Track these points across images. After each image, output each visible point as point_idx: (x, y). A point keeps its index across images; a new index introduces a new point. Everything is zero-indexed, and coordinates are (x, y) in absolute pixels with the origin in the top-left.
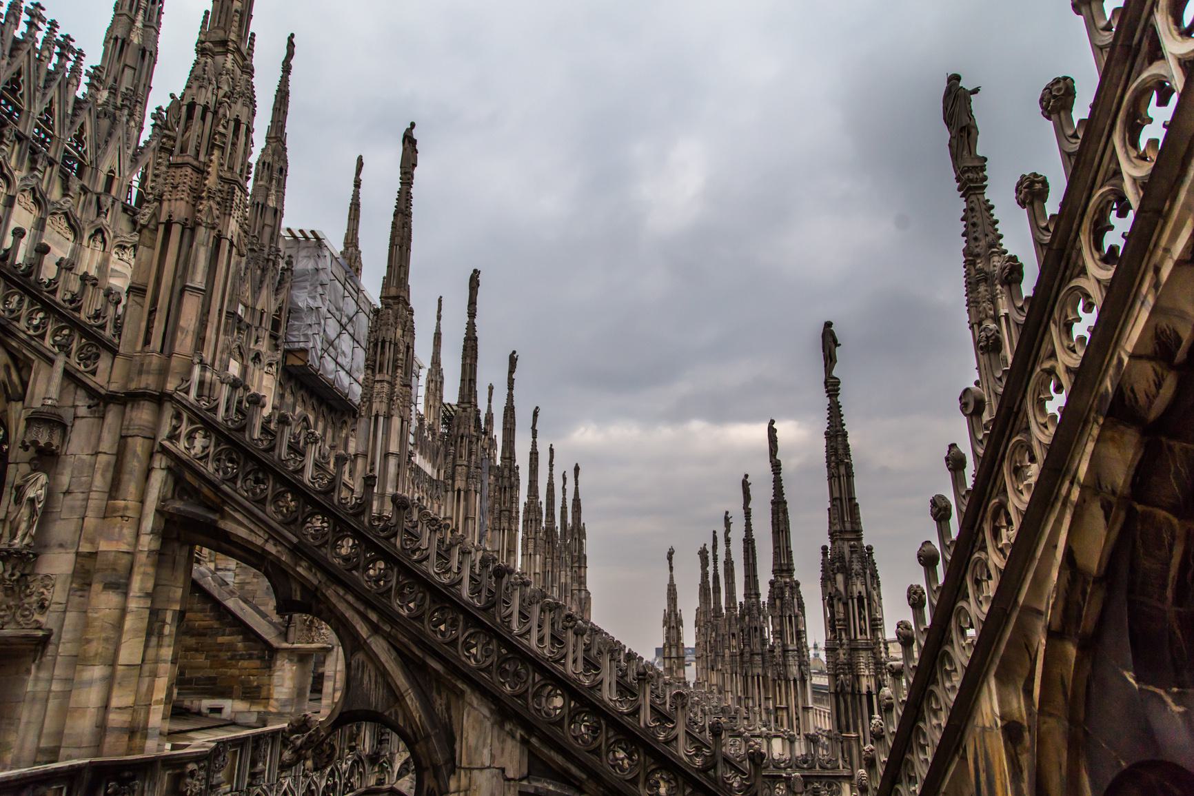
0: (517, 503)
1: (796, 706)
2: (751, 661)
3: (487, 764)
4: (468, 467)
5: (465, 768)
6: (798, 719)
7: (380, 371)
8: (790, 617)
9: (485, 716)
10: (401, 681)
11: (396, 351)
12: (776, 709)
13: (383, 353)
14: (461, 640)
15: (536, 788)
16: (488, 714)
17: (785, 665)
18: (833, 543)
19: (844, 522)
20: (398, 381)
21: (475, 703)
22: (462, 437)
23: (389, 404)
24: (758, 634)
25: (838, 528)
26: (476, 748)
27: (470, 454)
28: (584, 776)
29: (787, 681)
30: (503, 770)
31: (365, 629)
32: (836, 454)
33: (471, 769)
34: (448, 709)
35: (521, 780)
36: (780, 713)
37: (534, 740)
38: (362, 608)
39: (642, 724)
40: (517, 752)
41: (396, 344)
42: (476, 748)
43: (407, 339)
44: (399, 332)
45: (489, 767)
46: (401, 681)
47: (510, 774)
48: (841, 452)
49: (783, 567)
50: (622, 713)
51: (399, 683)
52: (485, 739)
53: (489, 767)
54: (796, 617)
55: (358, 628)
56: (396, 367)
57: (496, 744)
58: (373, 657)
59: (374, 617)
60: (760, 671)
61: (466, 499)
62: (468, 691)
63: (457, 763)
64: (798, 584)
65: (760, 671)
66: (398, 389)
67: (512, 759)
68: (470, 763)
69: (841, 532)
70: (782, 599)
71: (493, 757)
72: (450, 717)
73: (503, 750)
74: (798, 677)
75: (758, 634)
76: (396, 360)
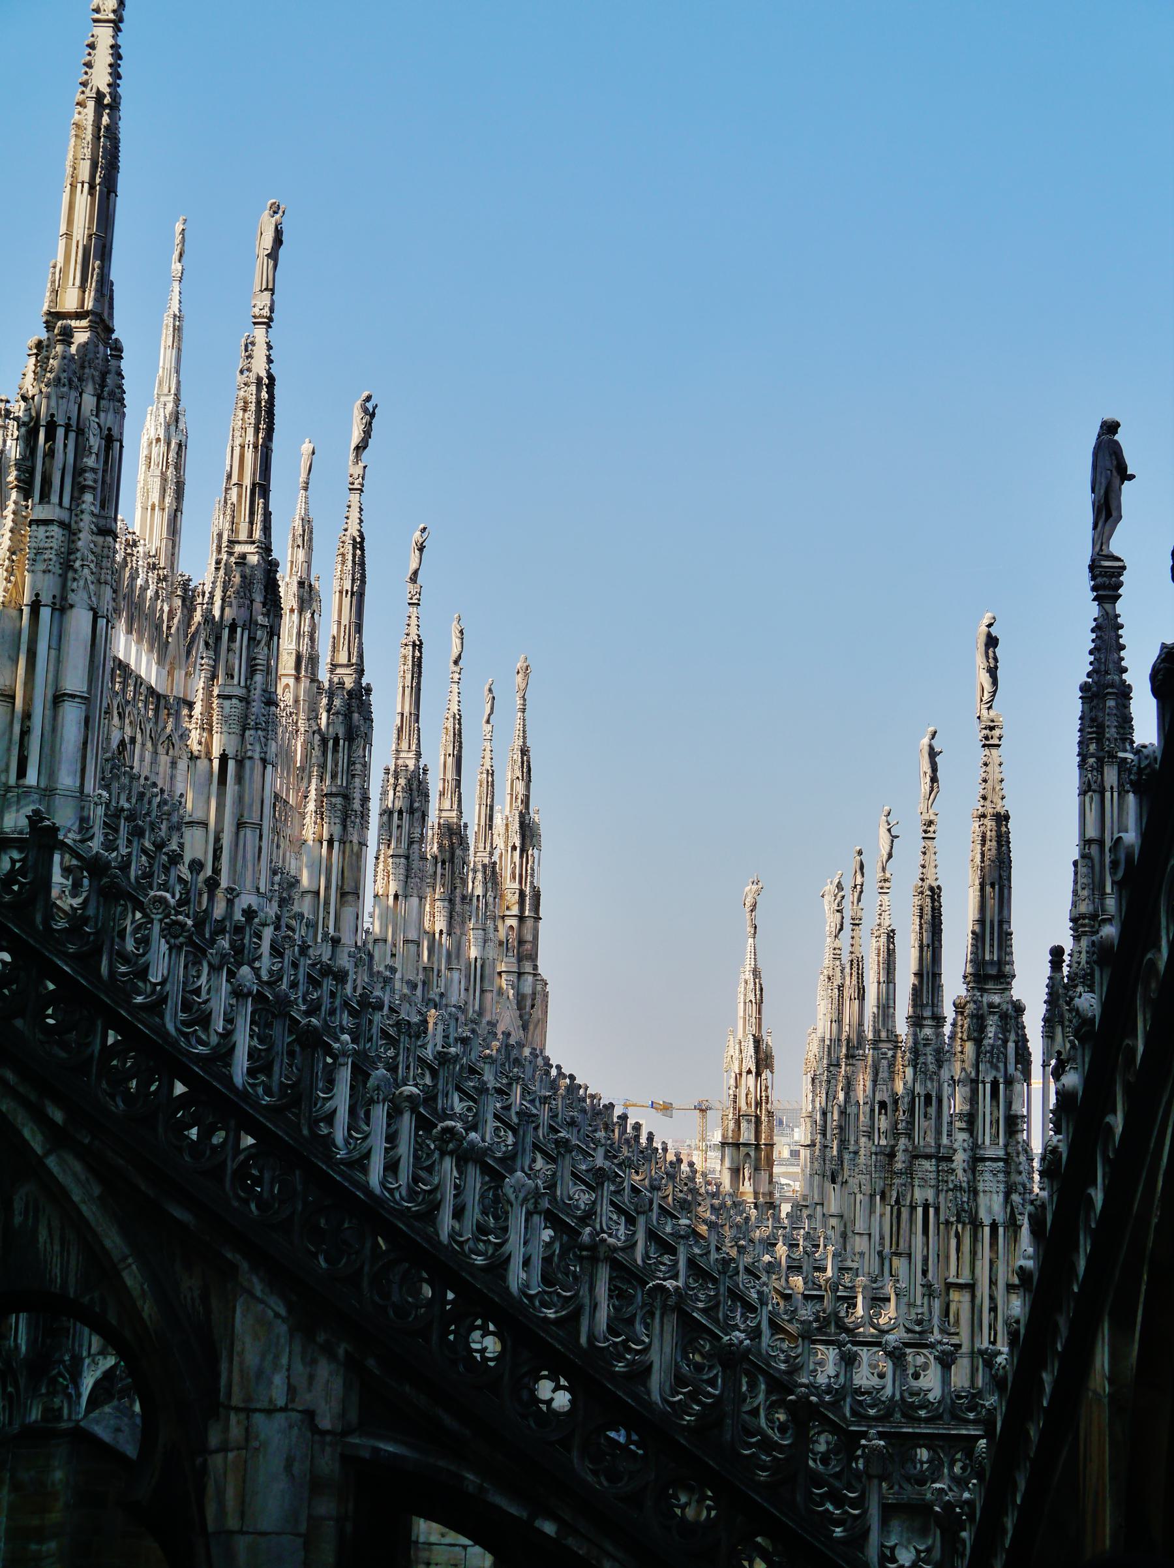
0: (365, 776)
1: (993, 1283)
2: (909, 1172)
3: (281, 1403)
4: (246, 700)
5: (238, 1410)
6: (993, 1309)
7: (44, 498)
8: (995, 1084)
9: (277, 1315)
10: (113, 1241)
11: (81, 450)
12: (949, 1286)
13: (50, 454)
14: (231, 1166)
17: (974, 1192)
18: (1077, 938)
19: (1103, 894)
20: (86, 523)
21: (258, 1289)
22: (233, 628)
23: (63, 577)
24: (932, 1111)
25: (1084, 908)
26: (260, 1373)
27: (252, 670)
29: (976, 1225)
31: (39, 1137)
32: (1100, 739)
33: (248, 1411)
35: (345, 1433)
36: (954, 1296)
37: (371, 1363)
38: (33, 1097)
39: (583, 1340)
40: (337, 1385)
41: (80, 432)
42: (260, 1373)
43: (107, 419)
44: (89, 401)
45: (283, 1409)
46: (113, 1241)
47: (325, 1423)
48: (1111, 733)
49: (991, 970)
50: (546, 1318)
51: (108, 1243)
52: (277, 1357)
53: (283, 1409)
54: (1009, 1082)
55: (27, 1134)
56: (79, 489)
57: (299, 1367)
58: (57, 1194)
59: (58, 1116)
60: (930, 1194)
61: (239, 779)
62: (245, 1266)
64: (1019, 1009)
65: (930, 1194)
66: (85, 539)
67: (328, 1392)
68: (248, 1399)
69: (1093, 917)
71: (291, 1391)
73: (311, 1378)
74: (1000, 1219)
75: (932, 1111)
76: (79, 471)
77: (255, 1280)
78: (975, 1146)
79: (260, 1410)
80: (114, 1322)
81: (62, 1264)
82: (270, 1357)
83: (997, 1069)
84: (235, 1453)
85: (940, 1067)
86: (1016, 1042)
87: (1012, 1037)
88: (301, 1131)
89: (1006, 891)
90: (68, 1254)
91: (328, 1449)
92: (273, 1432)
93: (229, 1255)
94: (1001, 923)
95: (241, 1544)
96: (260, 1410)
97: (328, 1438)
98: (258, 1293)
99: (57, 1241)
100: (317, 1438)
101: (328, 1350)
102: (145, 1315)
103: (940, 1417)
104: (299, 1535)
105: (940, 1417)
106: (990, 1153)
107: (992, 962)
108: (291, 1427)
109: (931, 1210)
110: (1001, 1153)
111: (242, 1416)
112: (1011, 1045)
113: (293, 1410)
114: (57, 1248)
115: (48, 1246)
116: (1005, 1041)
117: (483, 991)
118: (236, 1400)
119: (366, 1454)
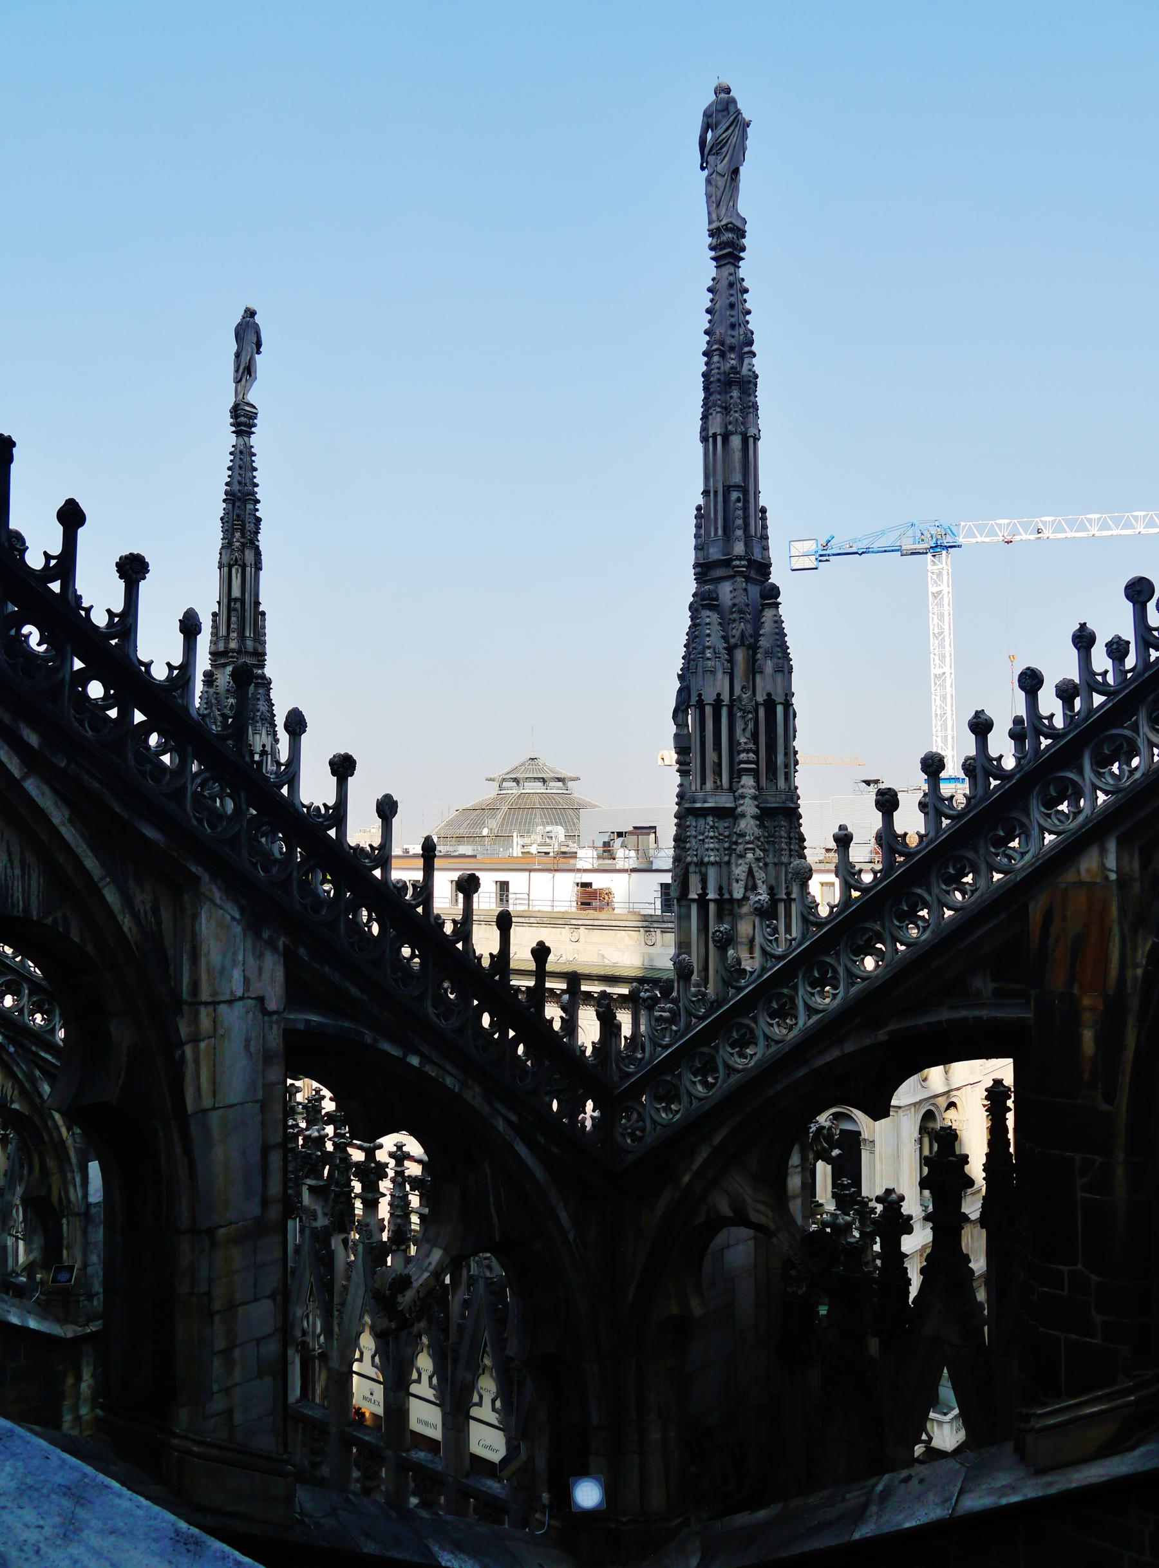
3: (239, 993)
5: (206, 1004)
9: (233, 918)
15: (308, 1022)
16: (238, 917)
21: (217, 895)
28: (365, 997)
30: (261, 1000)
33: (215, 1004)
34: (156, 910)
53: (241, 998)
57: (251, 960)
62: (206, 877)
63: (185, 995)
71: (246, 981)
72: (159, 922)
73: (260, 969)
77: (215, 890)
79: (224, 1002)
80: (77, 940)
81: (23, 887)
82: (229, 955)
84: (206, 1041)
88: (244, 757)
90: (30, 878)
91: (275, 1026)
92: (235, 1019)
93: (193, 869)
95: (215, 1118)
96: (224, 1002)
97: (275, 1017)
98: (218, 901)
99: (17, 863)
100: (266, 1018)
101: (271, 944)
102: (126, 928)
104: (257, 1101)
108: (247, 1012)
111: (210, 1008)
113: (248, 998)
114: (17, 872)
115: (9, 870)
118: (205, 996)
119: (301, 1026)
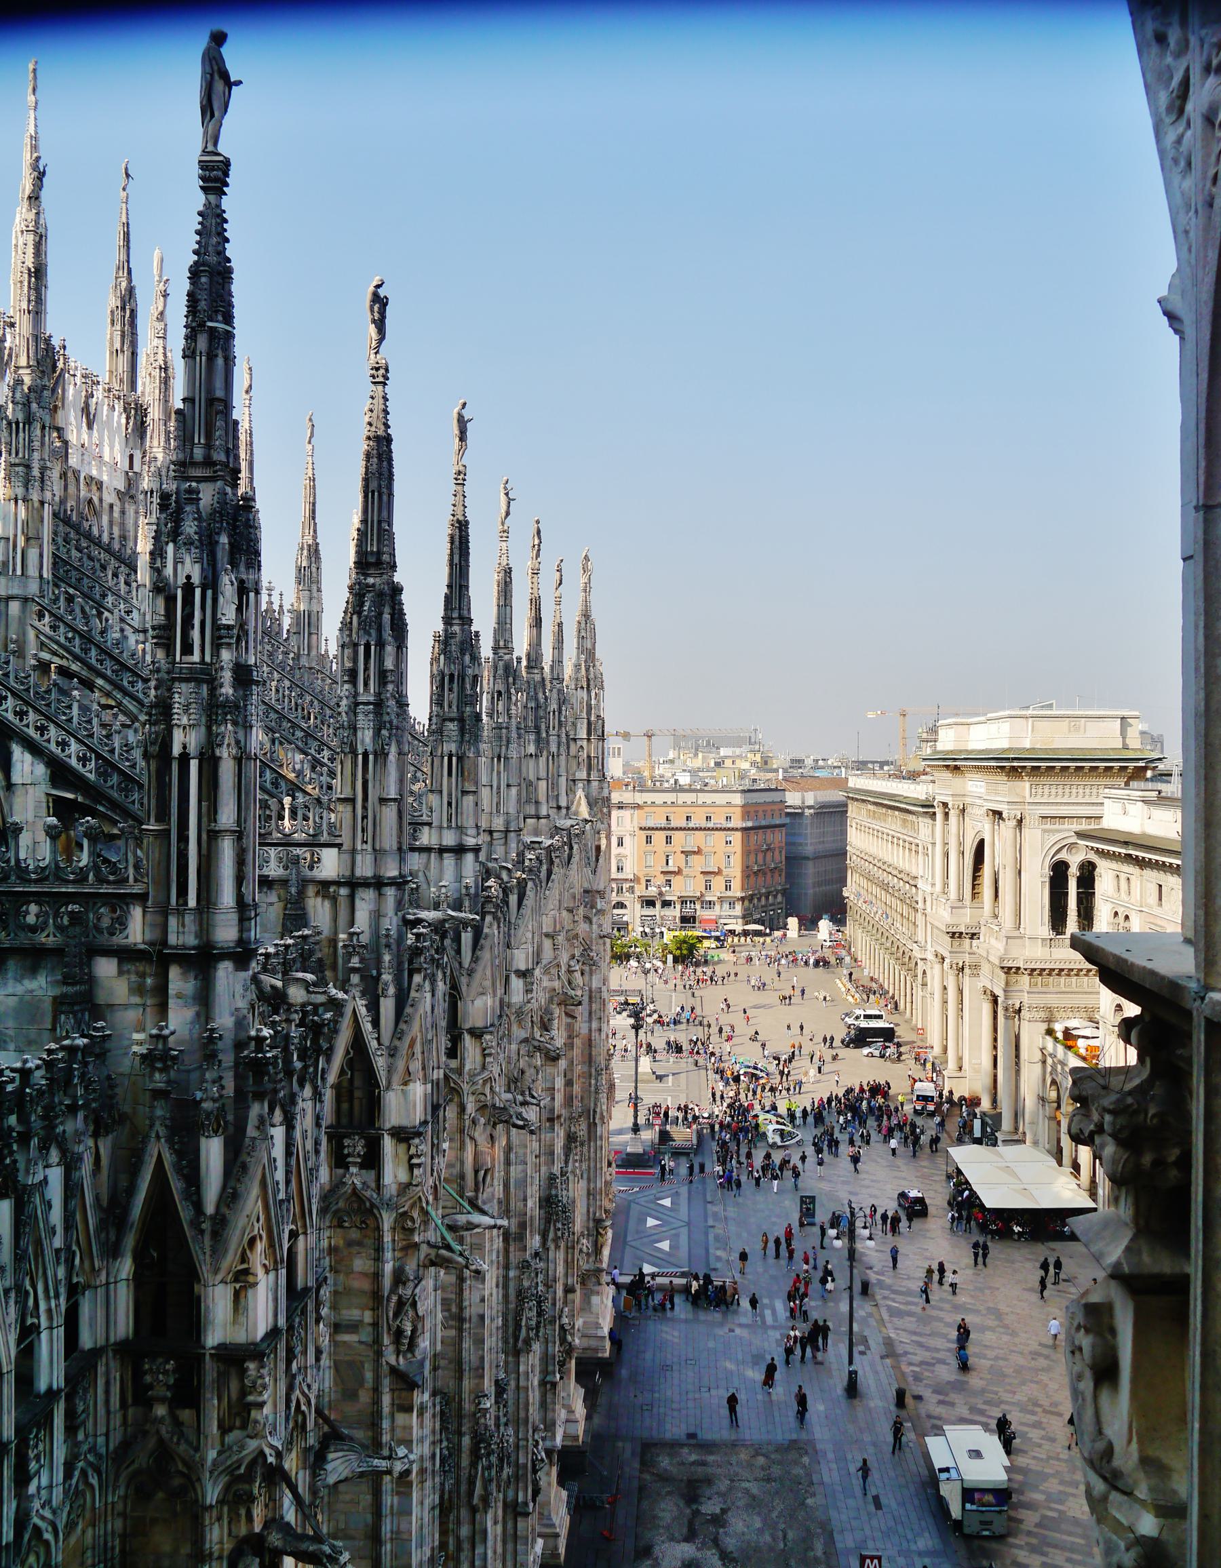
29: (354, 752)
70: (359, 613)
78: (356, 694)
83: (370, 635)
85: (463, 654)
86: (392, 615)
87: (387, 610)
89: (385, 498)
94: (380, 522)
103: (46, 878)
105: (46, 878)
106: (361, 699)
107: (372, 552)
109: (454, 759)
110: (372, 699)
112: (386, 617)
116: (380, 614)
117: (310, 634)
